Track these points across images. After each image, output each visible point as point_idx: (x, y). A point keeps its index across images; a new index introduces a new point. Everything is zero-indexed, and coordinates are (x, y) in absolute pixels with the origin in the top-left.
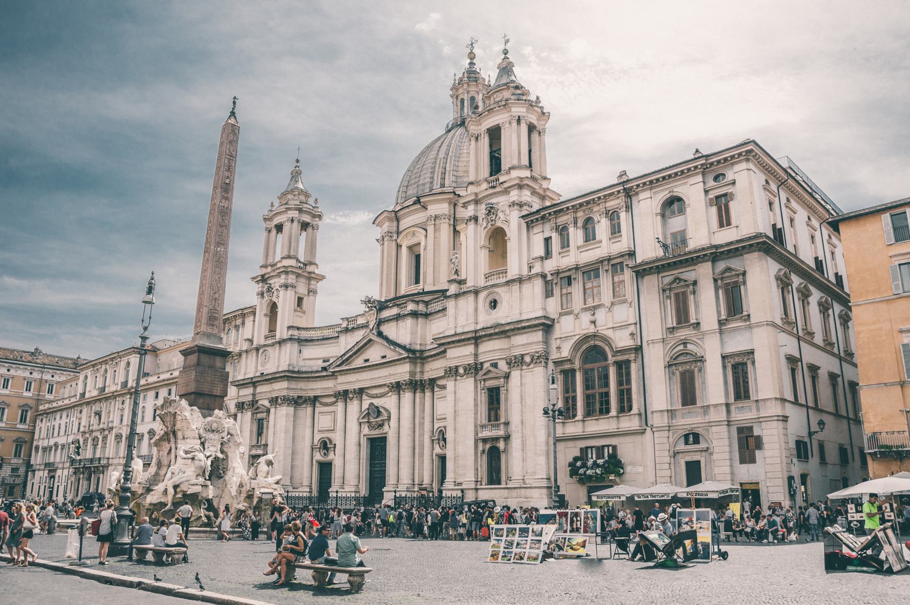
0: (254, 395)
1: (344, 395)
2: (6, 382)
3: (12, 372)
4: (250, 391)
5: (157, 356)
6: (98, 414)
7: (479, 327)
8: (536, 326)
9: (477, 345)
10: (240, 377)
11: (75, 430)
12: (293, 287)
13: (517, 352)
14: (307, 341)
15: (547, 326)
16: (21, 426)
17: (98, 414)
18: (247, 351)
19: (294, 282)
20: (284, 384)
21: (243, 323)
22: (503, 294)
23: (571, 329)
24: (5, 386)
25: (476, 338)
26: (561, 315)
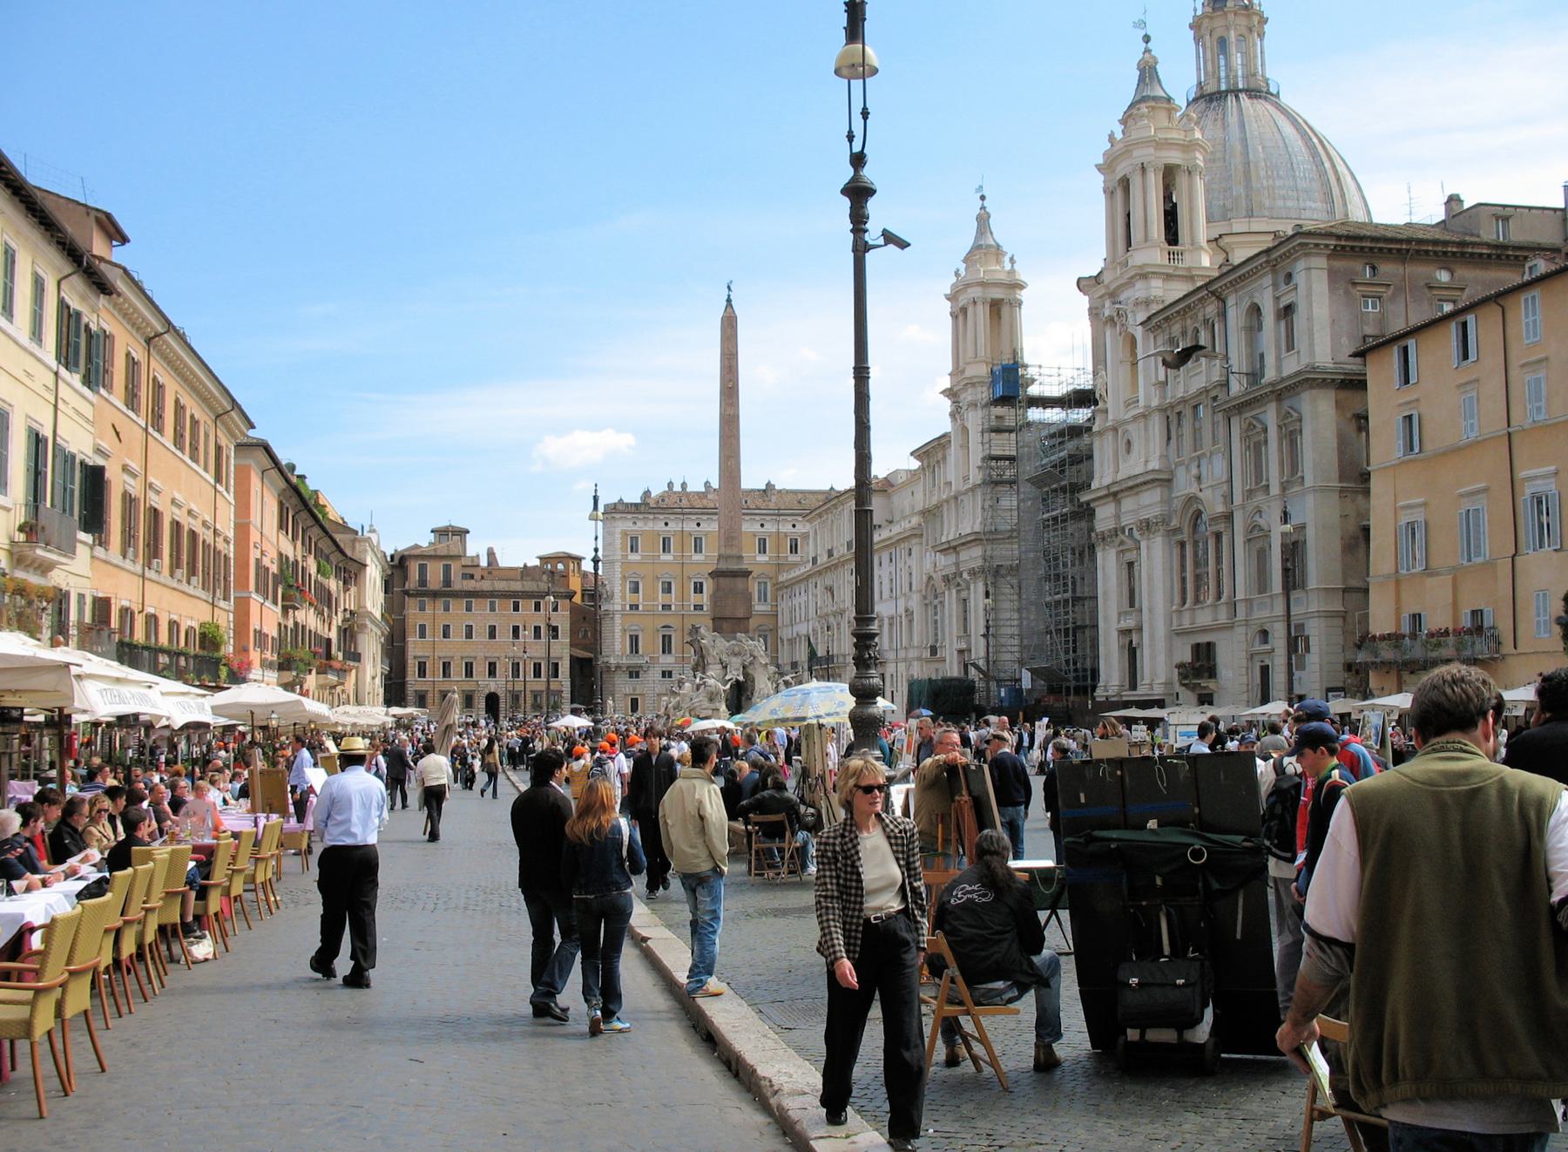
0: (957, 564)
4: (952, 558)
5: (889, 496)
6: (830, 590)
7: (1119, 478)
8: (1153, 481)
9: (1118, 502)
11: (812, 613)
13: (1144, 515)
17: (830, 590)
18: (947, 501)
20: (977, 552)
21: (944, 458)
22: (1135, 431)
23: (1184, 485)
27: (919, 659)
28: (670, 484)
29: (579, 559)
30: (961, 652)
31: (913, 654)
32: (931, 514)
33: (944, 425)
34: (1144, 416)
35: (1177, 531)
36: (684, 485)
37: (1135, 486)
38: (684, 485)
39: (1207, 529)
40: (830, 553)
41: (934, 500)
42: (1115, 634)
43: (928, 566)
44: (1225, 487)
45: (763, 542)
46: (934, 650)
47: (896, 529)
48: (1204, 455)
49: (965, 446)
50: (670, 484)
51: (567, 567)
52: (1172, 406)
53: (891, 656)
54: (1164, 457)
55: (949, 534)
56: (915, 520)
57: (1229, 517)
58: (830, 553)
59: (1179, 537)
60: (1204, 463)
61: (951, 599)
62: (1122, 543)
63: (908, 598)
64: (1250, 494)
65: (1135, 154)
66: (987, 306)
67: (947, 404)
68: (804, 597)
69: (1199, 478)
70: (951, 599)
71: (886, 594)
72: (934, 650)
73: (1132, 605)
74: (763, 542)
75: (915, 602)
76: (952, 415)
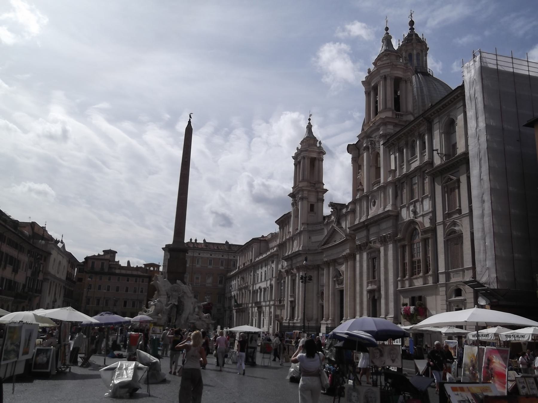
1: (328, 264)
2: (211, 261)
3: (213, 256)
4: (290, 262)
6: (243, 278)
10: (286, 255)
12: (307, 198)
14: (313, 231)
15: (397, 216)
16: (220, 286)
17: (243, 278)
18: (289, 239)
19: (306, 195)
24: (210, 264)
25: (366, 226)
26: (401, 208)
27: (274, 305)
28: (191, 240)
29: (158, 266)
30: (291, 302)
31: (272, 303)
32: (282, 246)
33: (289, 209)
34: (384, 188)
35: (400, 240)
36: (196, 240)
37: (378, 220)
38: (196, 240)
39: (418, 238)
40: (244, 264)
41: (284, 239)
42: (365, 293)
43: (280, 266)
44: (431, 215)
45: (222, 262)
46: (280, 301)
47: (269, 253)
48: (417, 201)
49: (297, 216)
50: (191, 240)
51: (154, 269)
52: (399, 180)
53: (263, 304)
54: (394, 205)
55: (288, 253)
56: (275, 249)
57: (433, 230)
58: (244, 264)
59: (403, 243)
60: (418, 205)
61: (288, 280)
62: (371, 248)
63: (271, 280)
64: (447, 216)
65: (382, 72)
66: (309, 158)
67: (291, 200)
68: (235, 282)
69: (415, 212)
70: (288, 280)
71: (263, 280)
72: (280, 301)
73: (374, 278)
74: (222, 262)
75: (273, 282)
76: (293, 204)
